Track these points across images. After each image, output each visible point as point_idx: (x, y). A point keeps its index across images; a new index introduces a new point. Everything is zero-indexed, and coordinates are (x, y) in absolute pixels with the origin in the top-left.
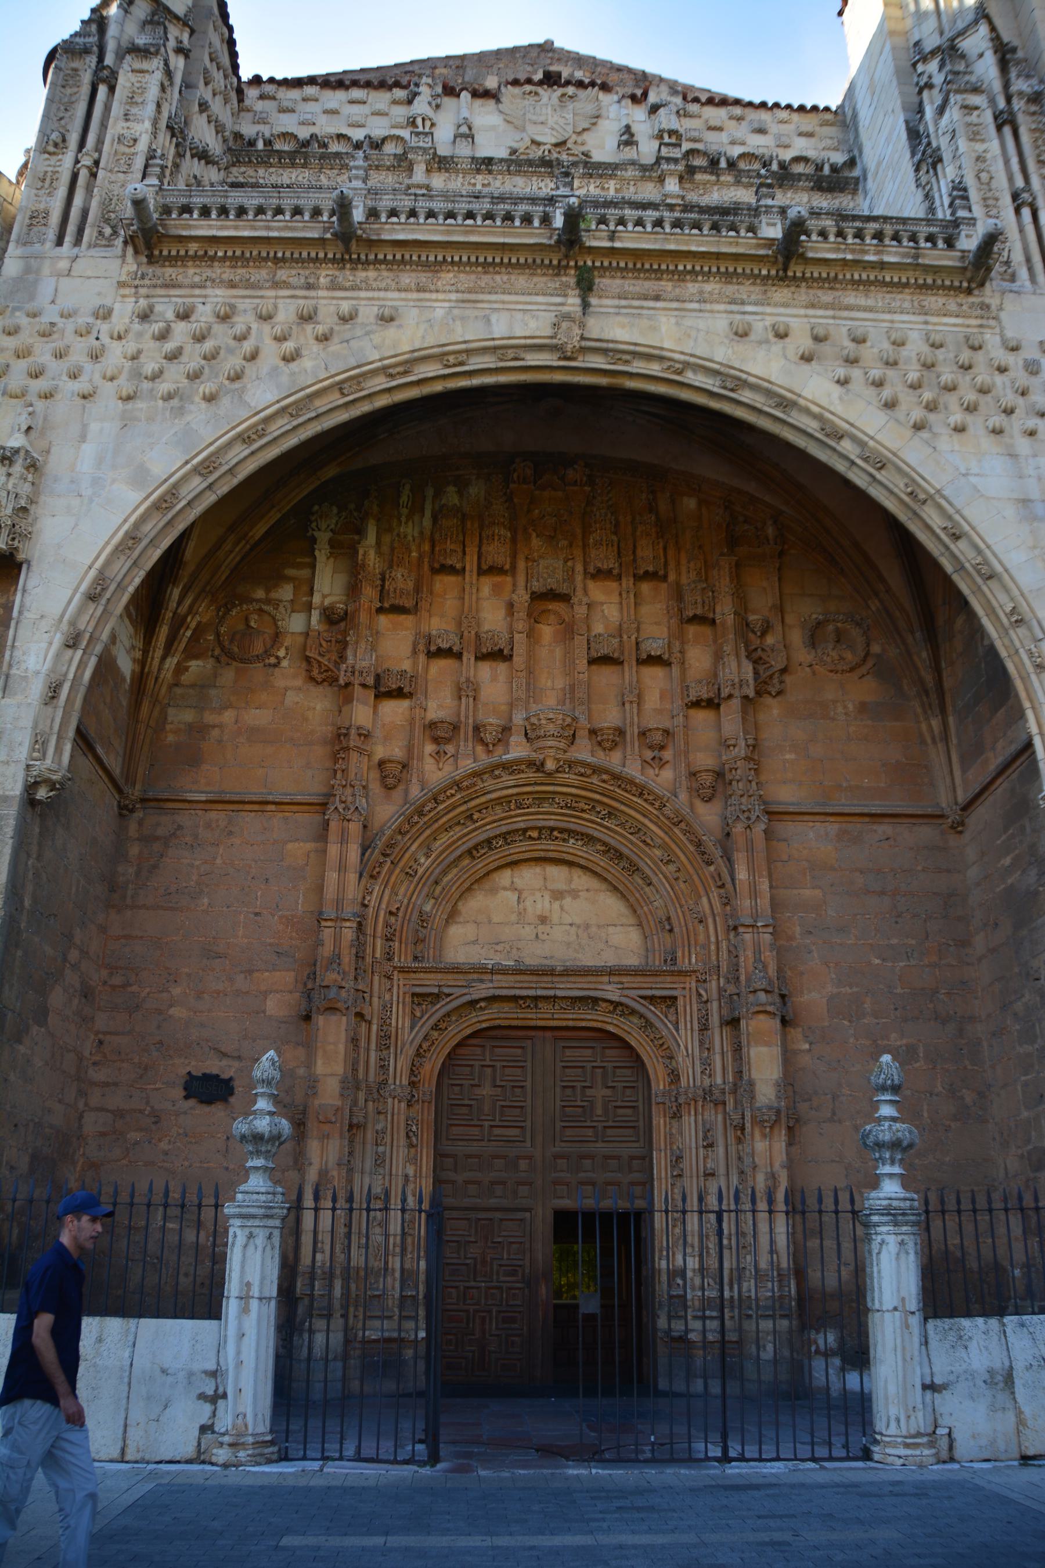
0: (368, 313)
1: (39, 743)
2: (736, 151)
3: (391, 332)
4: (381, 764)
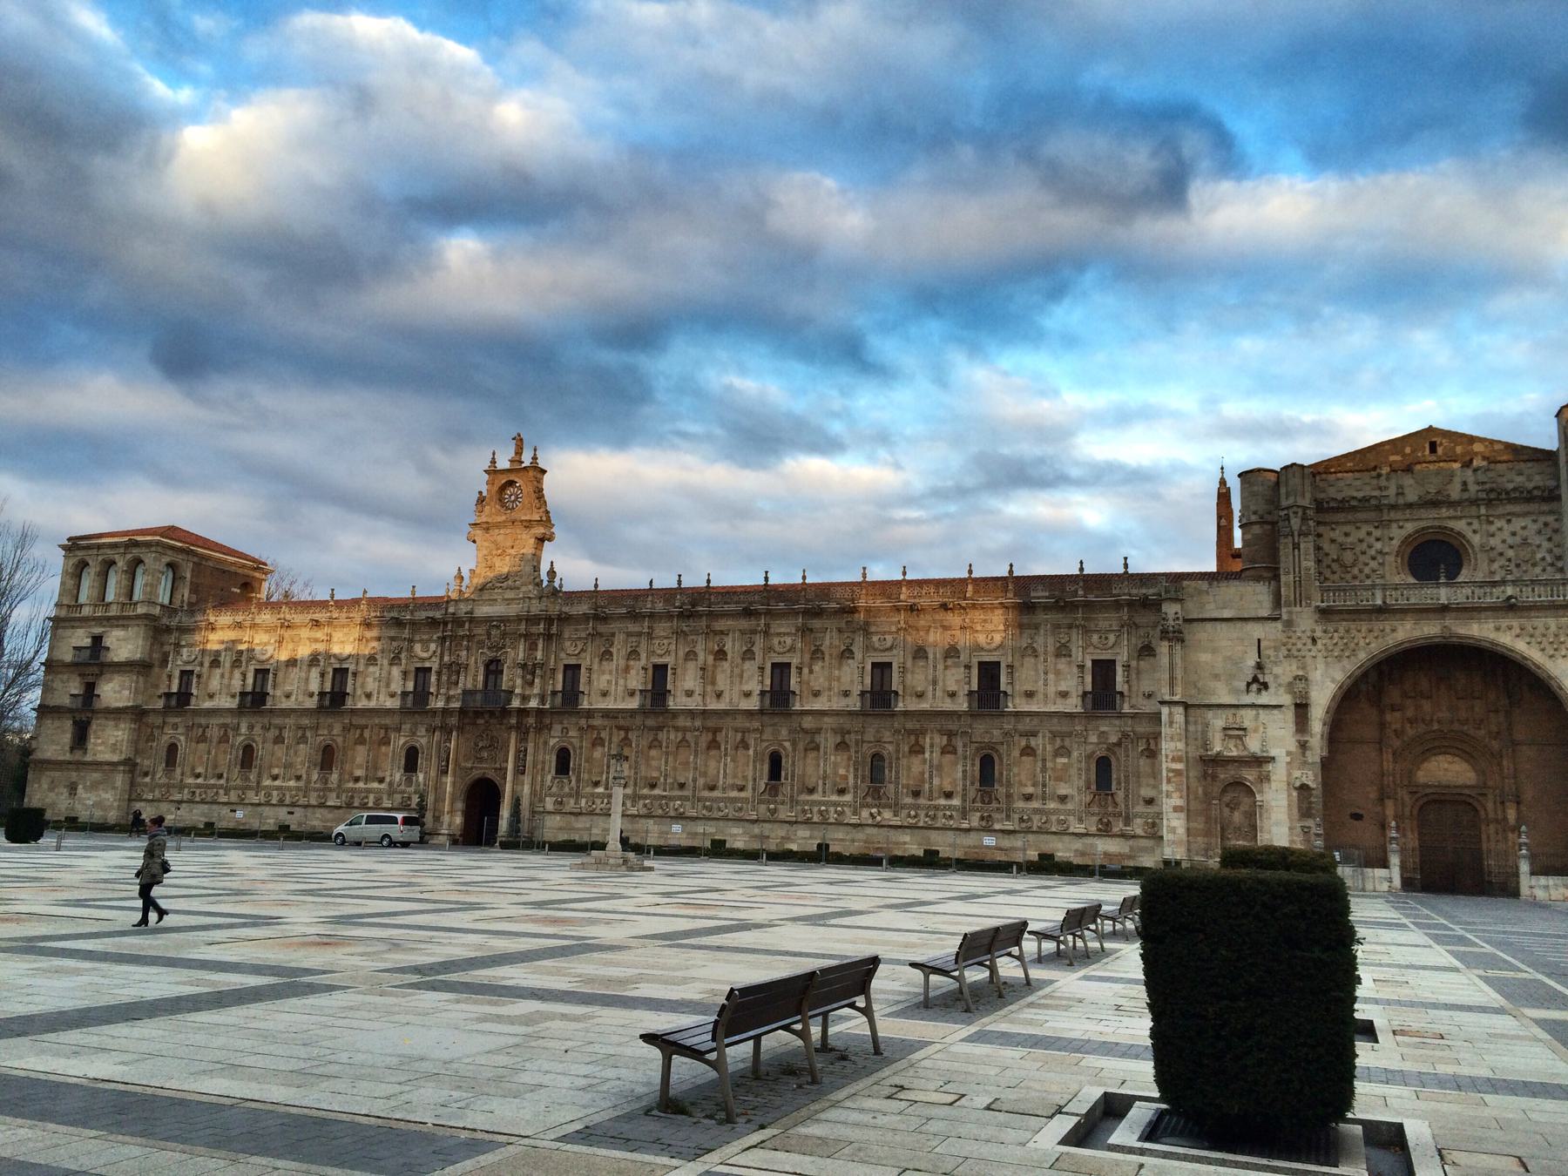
0: (1388, 629)
1: (1322, 749)
2: (1511, 486)
3: (1395, 634)
4: (1395, 731)
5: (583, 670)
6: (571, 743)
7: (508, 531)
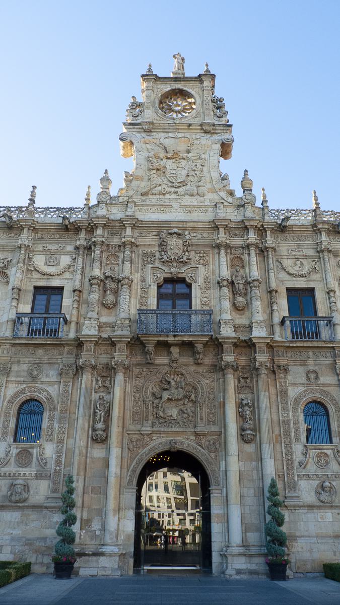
5: (320, 296)
6: (325, 393)
7: (180, 135)
